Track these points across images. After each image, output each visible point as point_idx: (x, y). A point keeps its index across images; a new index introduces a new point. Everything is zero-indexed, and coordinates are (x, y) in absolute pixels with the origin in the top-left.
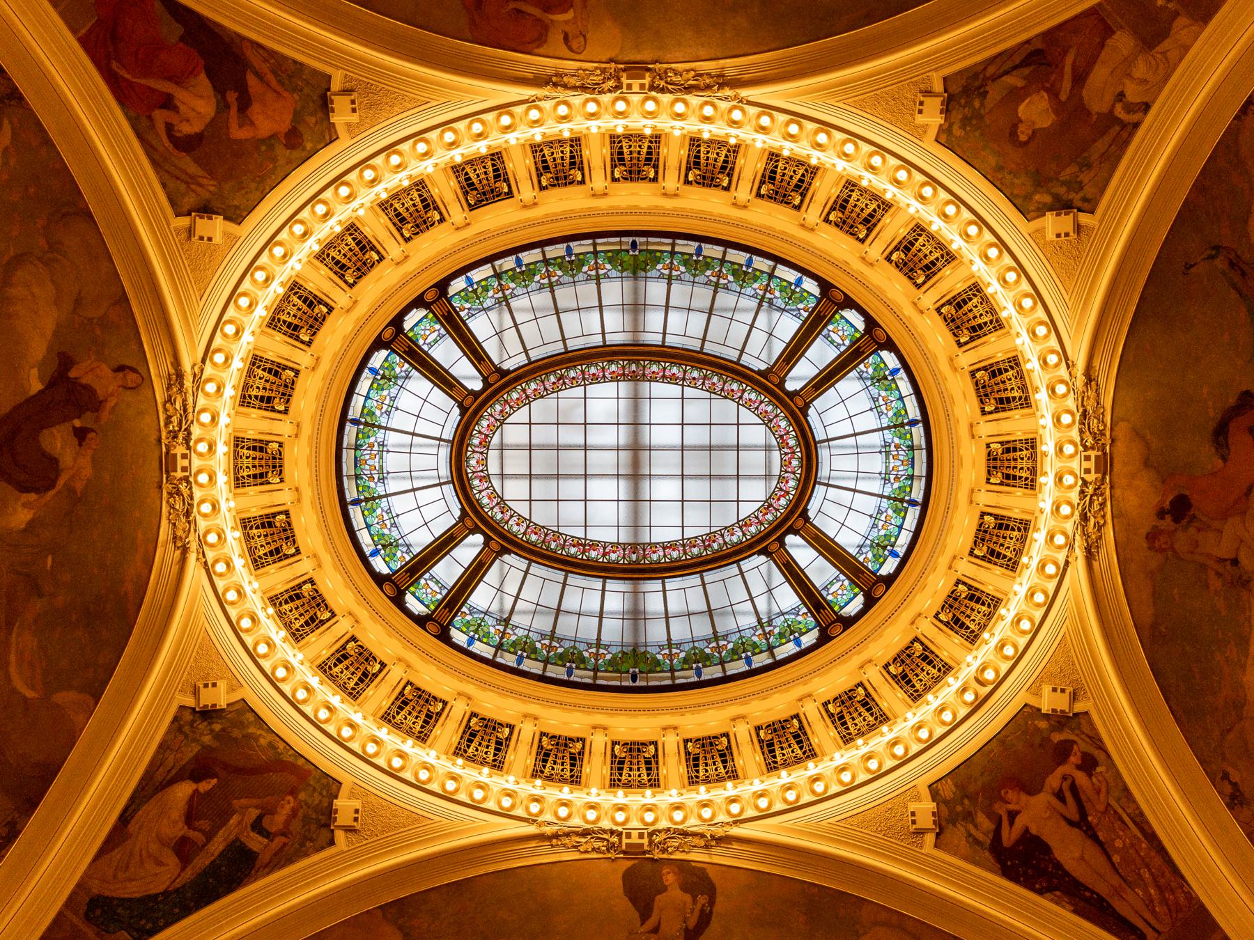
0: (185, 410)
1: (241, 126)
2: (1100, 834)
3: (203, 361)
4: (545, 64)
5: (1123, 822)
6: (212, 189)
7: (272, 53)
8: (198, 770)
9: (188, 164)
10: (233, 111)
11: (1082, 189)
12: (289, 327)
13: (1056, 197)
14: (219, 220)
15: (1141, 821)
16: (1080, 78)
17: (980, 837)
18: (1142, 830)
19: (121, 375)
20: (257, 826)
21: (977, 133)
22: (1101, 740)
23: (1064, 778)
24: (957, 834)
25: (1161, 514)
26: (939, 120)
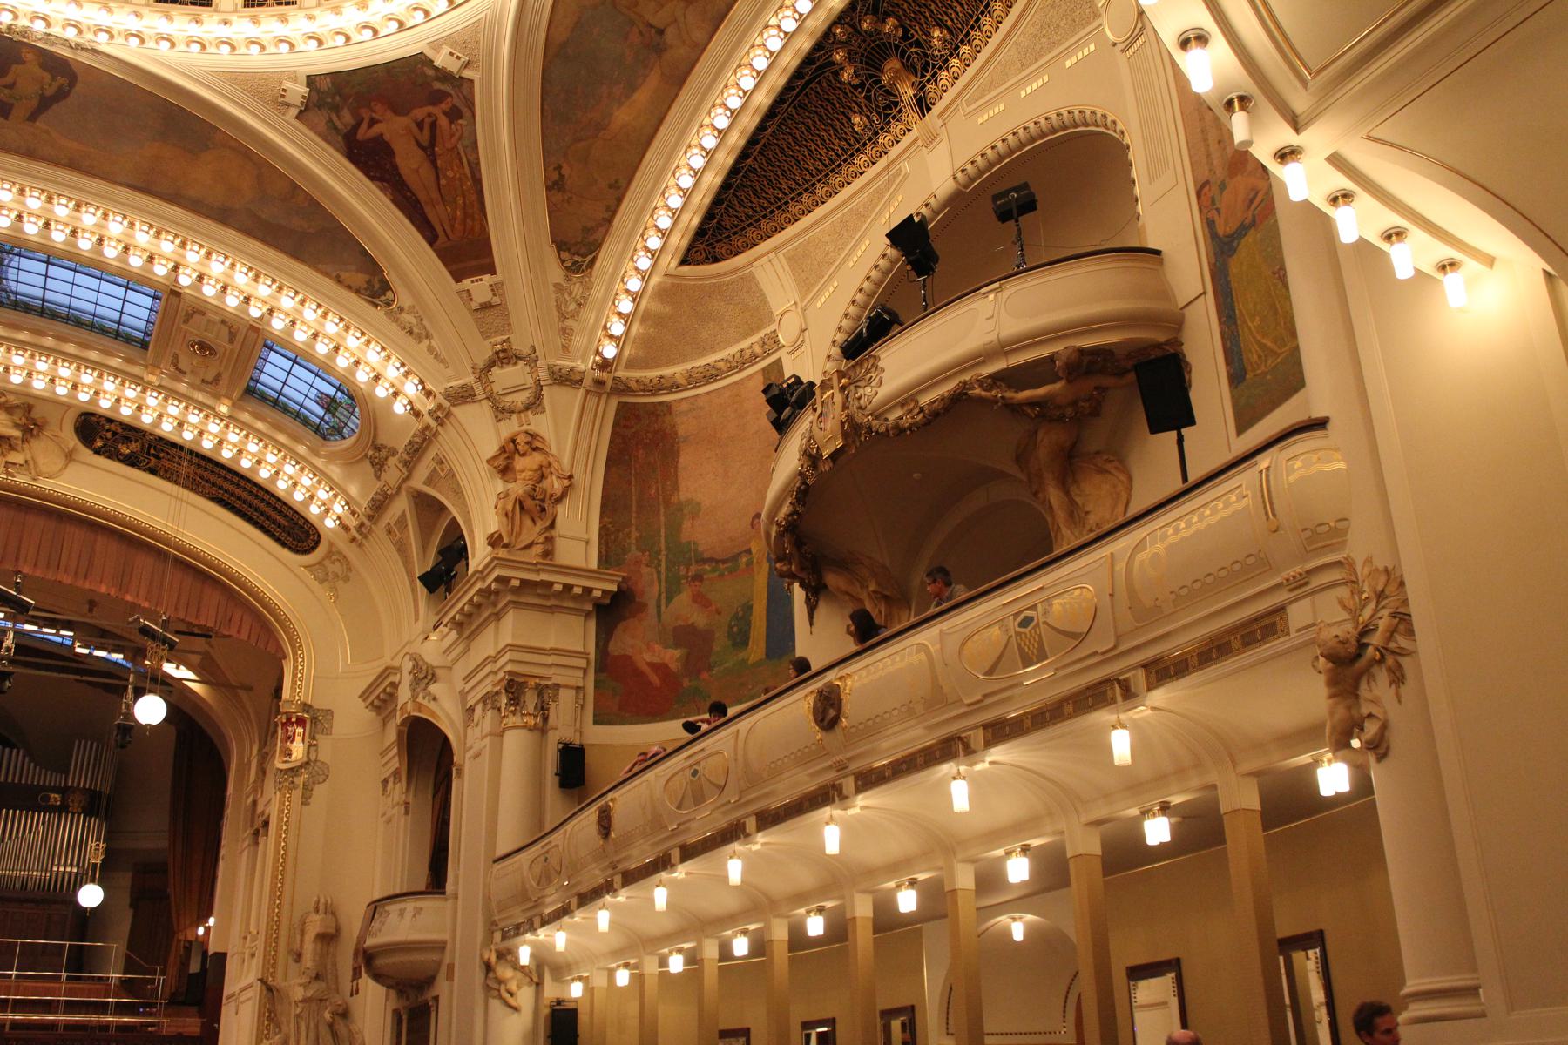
15: (475, 168)
17: (339, 125)
18: (473, 175)
24: (320, 118)
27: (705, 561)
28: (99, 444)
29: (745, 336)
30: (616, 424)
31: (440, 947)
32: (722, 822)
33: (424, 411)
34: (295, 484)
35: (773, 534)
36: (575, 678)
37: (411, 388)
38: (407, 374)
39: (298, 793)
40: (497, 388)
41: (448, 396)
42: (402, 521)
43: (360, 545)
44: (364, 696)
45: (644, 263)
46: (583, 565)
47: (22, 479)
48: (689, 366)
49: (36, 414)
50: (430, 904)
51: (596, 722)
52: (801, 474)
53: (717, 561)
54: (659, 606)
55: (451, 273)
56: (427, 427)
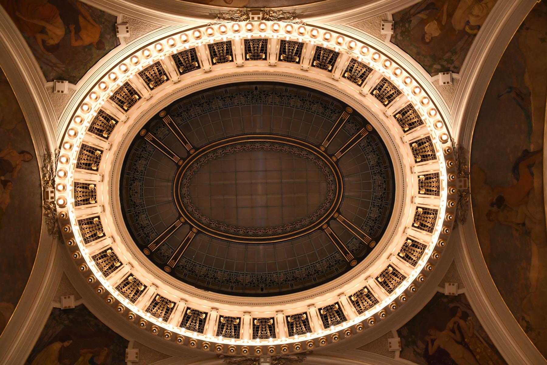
0: (52, 171)
1: (76, 40)
2: (470, 347)
3: (60, 148)
4: (215, 8)
5: (481, 341)
6: (63, 69)
7: (91, 7)
9: (53, 58)
10: (73, 34)
11: (453, 63)
12: (98, 131)
13: (443, 66)
14: (66, 83)
16: (450, 15)
17: (418, 350)
19: (22, 155)
21: (408, 38)
22: (470, 306)
23: (455, 323)
25: (492, 205)
26: (391, 33)
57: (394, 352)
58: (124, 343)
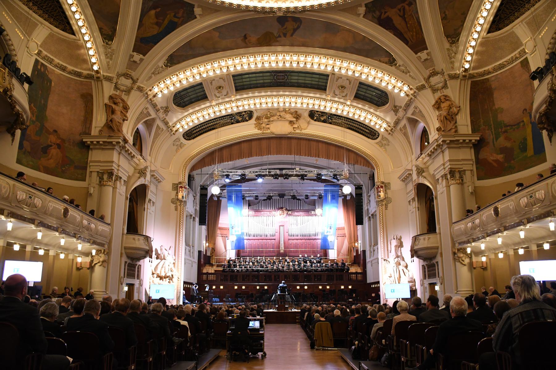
8: (154, 7)
20: (175, 16)
27: (507, 126)
28: (315, 118)
29: (512, 52)
30: (471, 88)
31: (437, 248)
32: (543, 211)
33: (410, 94)
34: (371, 120)
35: (537, 116)
36: (469, 167)
37: (406, 88)
38: (404, 84)
39: (384, 207)
40: (432, 84)
41: (417, 89)
42: (405, 126)
43: (392, 135)
44: (399, 178)
45: (476, 36)
46: (467, 133)
47: (297, 131)
48: (493, 65)
49: (298, 113)
50: (431, 236)
51: (478, 180)
52: (550, 96)
53: (512, 126)
54: (493, 142)
55: (414, 52)
56: (411, 99)
57: (360, 14)
58: (192, 6)
